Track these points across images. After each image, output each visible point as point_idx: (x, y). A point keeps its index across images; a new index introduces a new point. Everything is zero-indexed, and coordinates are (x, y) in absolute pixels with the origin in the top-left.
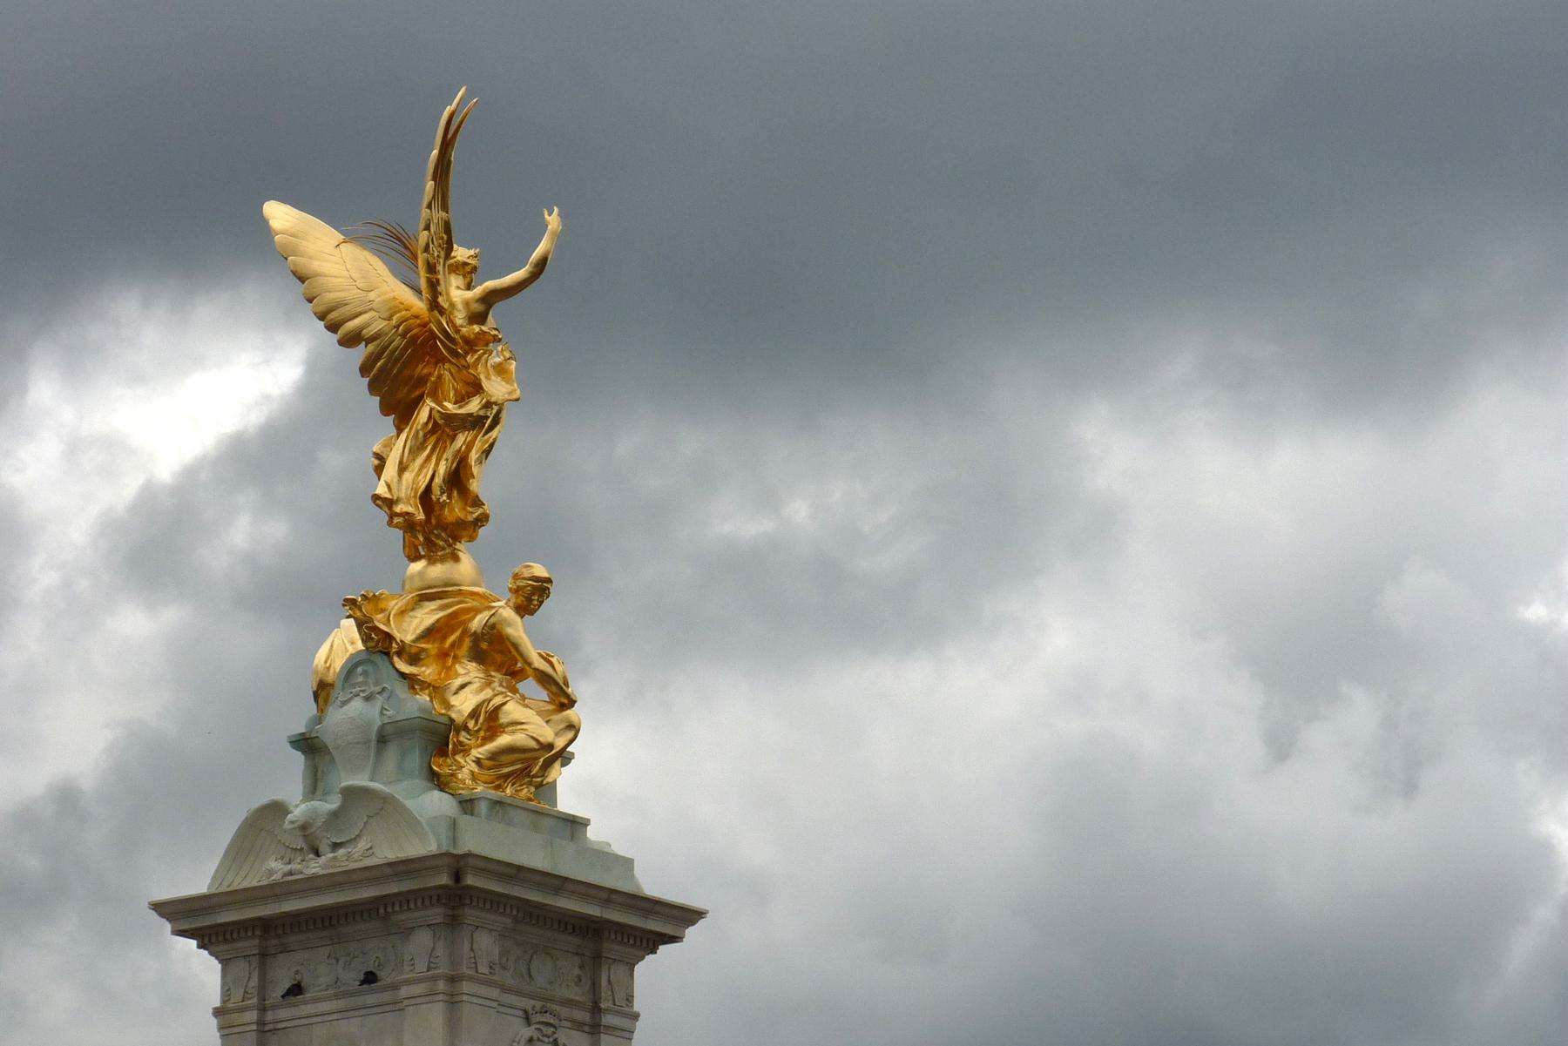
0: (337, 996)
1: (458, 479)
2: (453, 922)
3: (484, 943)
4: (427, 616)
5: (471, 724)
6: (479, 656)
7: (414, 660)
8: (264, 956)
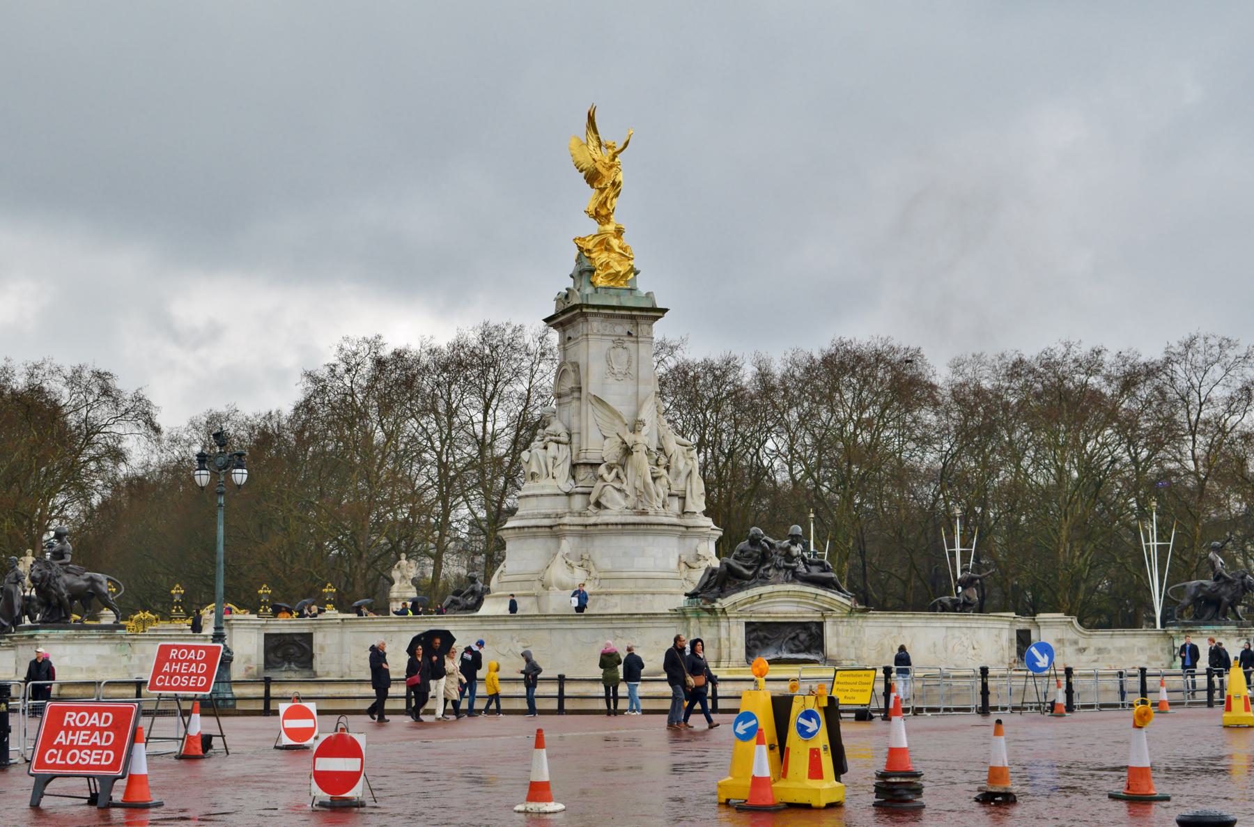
3: (595, 325)
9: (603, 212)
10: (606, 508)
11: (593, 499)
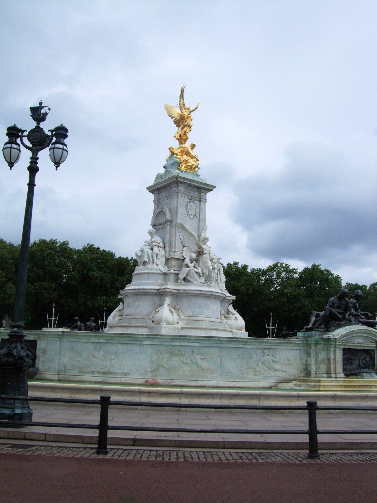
0: (166, 197)
1: (185, 134)
2: (178, 186)
4: (180, 150)
5: (183, 162)
6: (186, 155)
7: (177, 155)
8: (159, 194)
9: (184, 138)
10: (189, 281)
11: (181, 277)
